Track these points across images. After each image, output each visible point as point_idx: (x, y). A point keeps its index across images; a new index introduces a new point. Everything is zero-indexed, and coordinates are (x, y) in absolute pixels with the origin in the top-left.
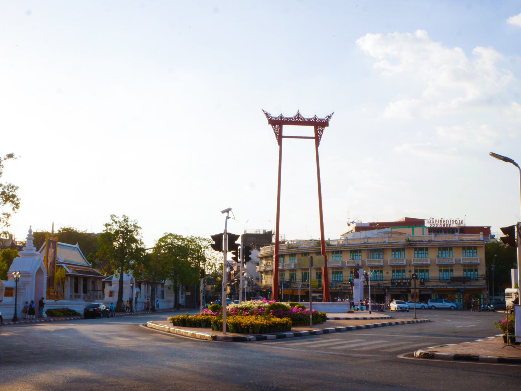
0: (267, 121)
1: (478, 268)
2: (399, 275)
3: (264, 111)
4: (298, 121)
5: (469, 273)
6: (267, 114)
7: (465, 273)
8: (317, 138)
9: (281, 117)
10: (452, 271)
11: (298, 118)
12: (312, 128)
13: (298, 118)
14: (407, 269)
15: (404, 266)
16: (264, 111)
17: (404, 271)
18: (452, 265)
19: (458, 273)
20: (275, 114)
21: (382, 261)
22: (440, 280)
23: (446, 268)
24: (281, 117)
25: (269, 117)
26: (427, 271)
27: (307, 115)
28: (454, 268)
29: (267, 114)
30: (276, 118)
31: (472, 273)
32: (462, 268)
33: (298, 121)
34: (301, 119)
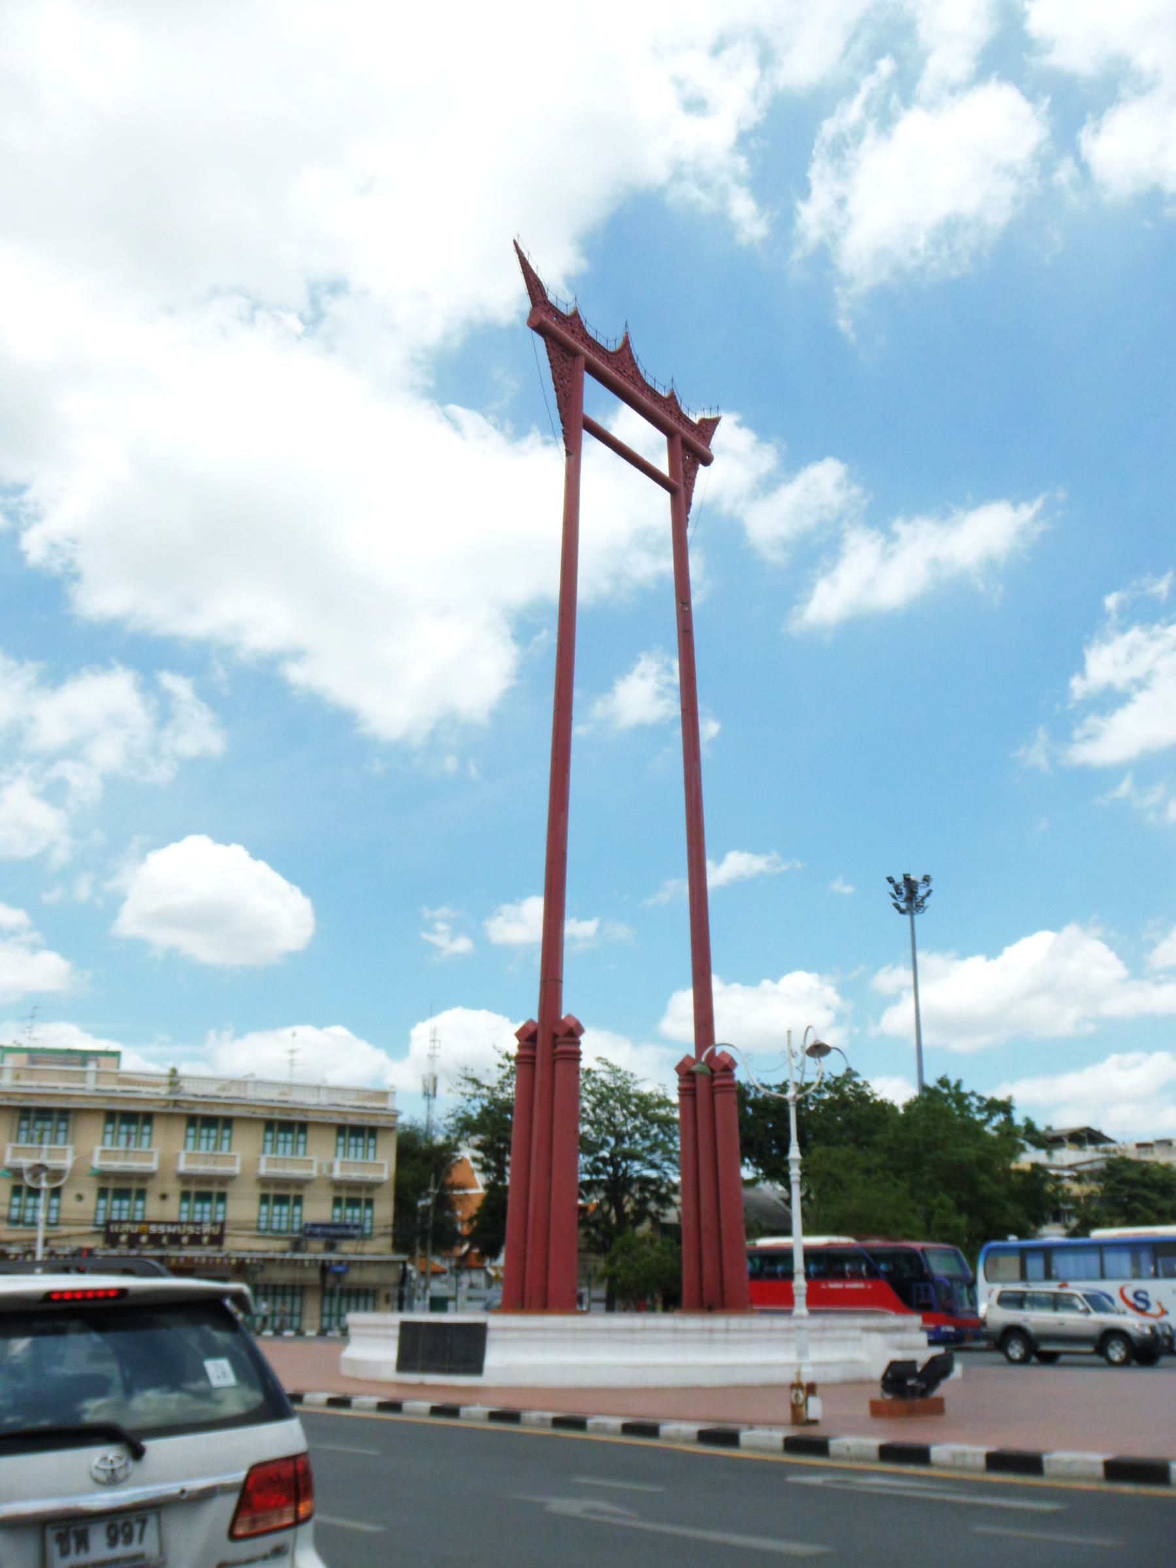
1: (377, 1195)
2: (121, 1209)
5: (349, 1212)
7: (337, 1212)
10: (298, 1200)
14: (154, 1189)
15: (144, 1177)
17: (141, 1194)
18: (301, 1183)
19: (318, 1210)
21: (70, 1153)
22: (265, 1232)
23: (281, 1193)
26: (222, 1197)
28: (306, 1192)
31: (357, 1212)
32: (330, 1194)
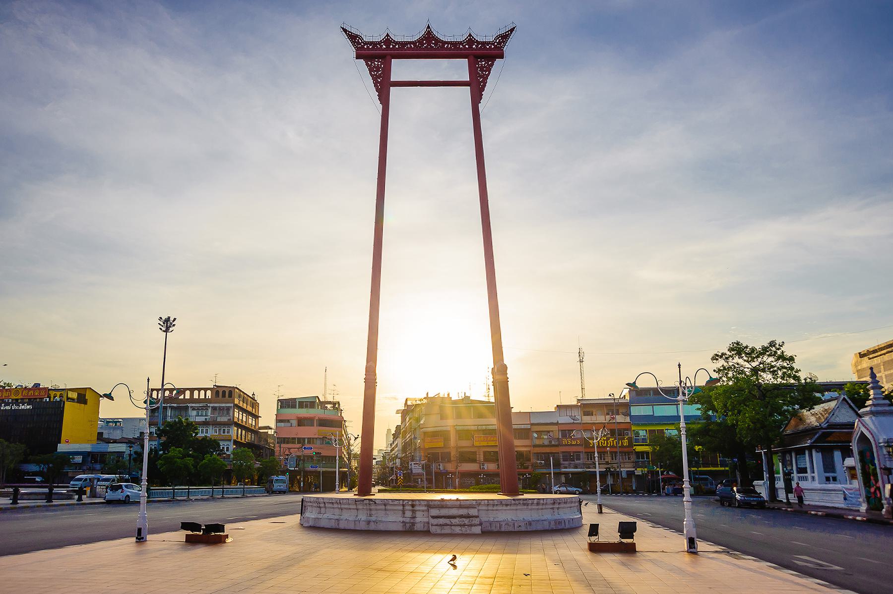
0: (352, 51)
3: (345, 30)
4: (429, 47)
6: (353, 38)
8: (477, 85)
9: (388, 41)
11: (429, 43)
12: (465, 62)
13: (429, 43)
16: (345, 30)
20: (372, 34)
24: (388, 41)
25: (359, 43)
27: (450, 32)
29: (353, 38)
30: (374, 44)
33: (429, 47)
34: (436, 44)
